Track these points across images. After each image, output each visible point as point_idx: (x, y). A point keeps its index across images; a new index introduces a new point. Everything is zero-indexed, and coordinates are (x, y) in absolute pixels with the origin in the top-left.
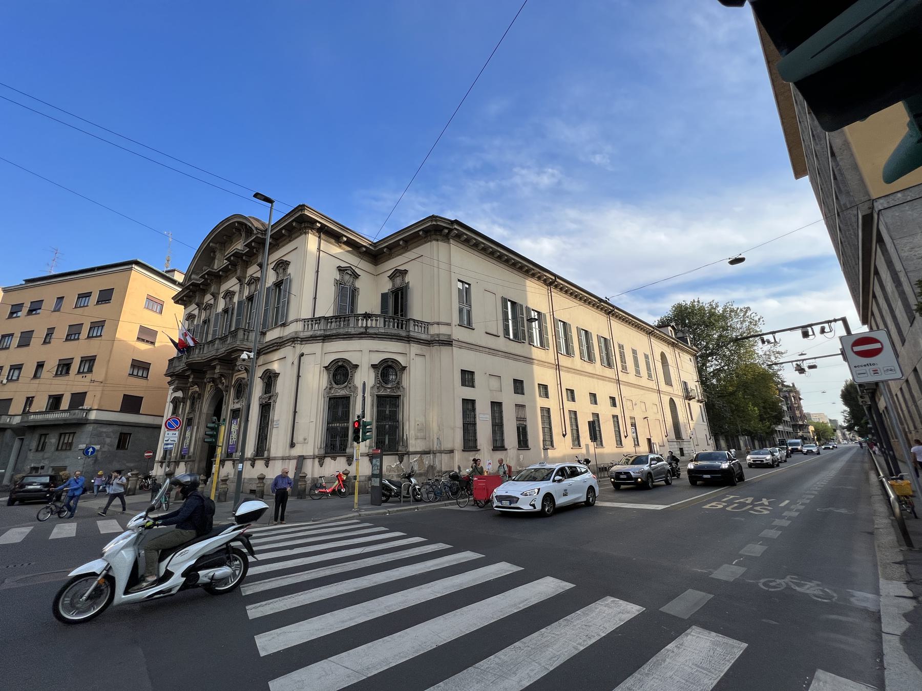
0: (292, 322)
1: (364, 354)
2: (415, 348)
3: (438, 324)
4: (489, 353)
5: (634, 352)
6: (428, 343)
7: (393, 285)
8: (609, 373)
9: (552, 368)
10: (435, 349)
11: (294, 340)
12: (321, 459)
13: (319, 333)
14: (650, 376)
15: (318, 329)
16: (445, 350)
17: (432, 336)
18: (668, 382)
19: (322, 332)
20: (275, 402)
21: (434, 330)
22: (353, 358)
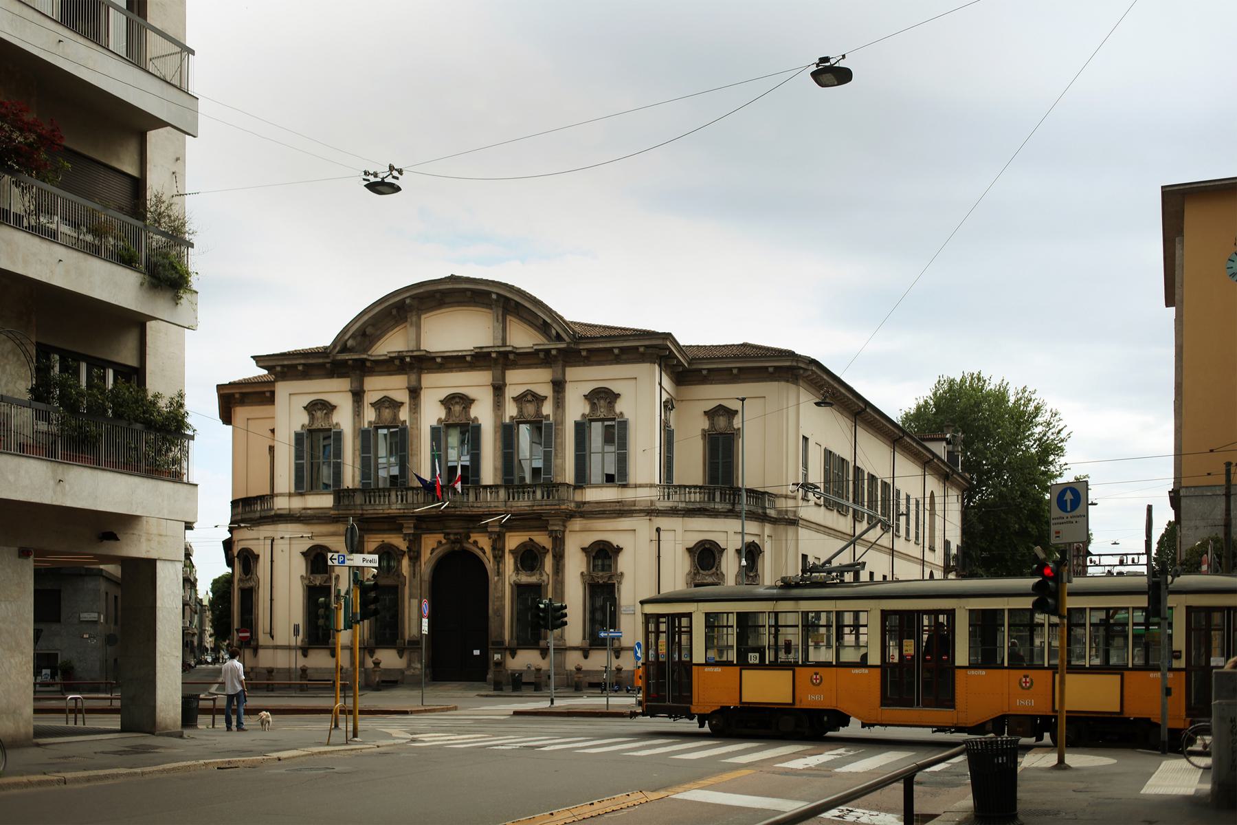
0: (641, 486)
1: (728, 534)
2: (768, 529)
3: (786, 497)
4: (825, 533)
5: (908, 498)
6: (774, 521)
7: (712, 424)
8: (886, 541)
9: (885, 553)
10: (781, 527)
11: (651, 512)
12: (305, 651)
13: (681, 505)
14: (917, 538)
15: (676, 501)
16: (791, 529)
17: (779, 512)
18: (932, 549)
19: (684, 505)
20: (620, 583)
21: (782, 504)
22: (720, 540)
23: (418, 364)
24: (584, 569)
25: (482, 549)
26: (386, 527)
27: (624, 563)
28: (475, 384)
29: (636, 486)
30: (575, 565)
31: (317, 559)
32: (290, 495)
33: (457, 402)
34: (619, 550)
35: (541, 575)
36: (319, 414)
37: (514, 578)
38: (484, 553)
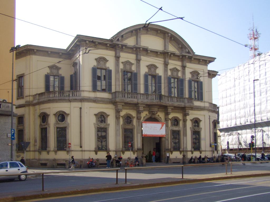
23: (139, 51)
24: (191, 126)
25: (161, 118)
26: (128, 107)
27: (202, 125)
28: (158, 62)
29: (205, 102)
30: (189, 124)
31: (102, 117)
32: (89, 91)
33: (152, 67)
34: (200, 121)
35: (179, 127)
36: (101, 62)
37: (171, 128)
38: (161, 119)
